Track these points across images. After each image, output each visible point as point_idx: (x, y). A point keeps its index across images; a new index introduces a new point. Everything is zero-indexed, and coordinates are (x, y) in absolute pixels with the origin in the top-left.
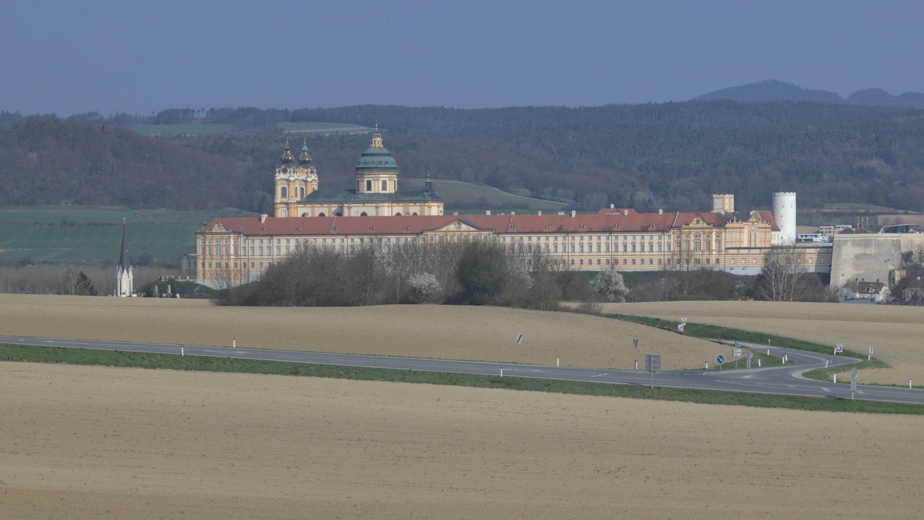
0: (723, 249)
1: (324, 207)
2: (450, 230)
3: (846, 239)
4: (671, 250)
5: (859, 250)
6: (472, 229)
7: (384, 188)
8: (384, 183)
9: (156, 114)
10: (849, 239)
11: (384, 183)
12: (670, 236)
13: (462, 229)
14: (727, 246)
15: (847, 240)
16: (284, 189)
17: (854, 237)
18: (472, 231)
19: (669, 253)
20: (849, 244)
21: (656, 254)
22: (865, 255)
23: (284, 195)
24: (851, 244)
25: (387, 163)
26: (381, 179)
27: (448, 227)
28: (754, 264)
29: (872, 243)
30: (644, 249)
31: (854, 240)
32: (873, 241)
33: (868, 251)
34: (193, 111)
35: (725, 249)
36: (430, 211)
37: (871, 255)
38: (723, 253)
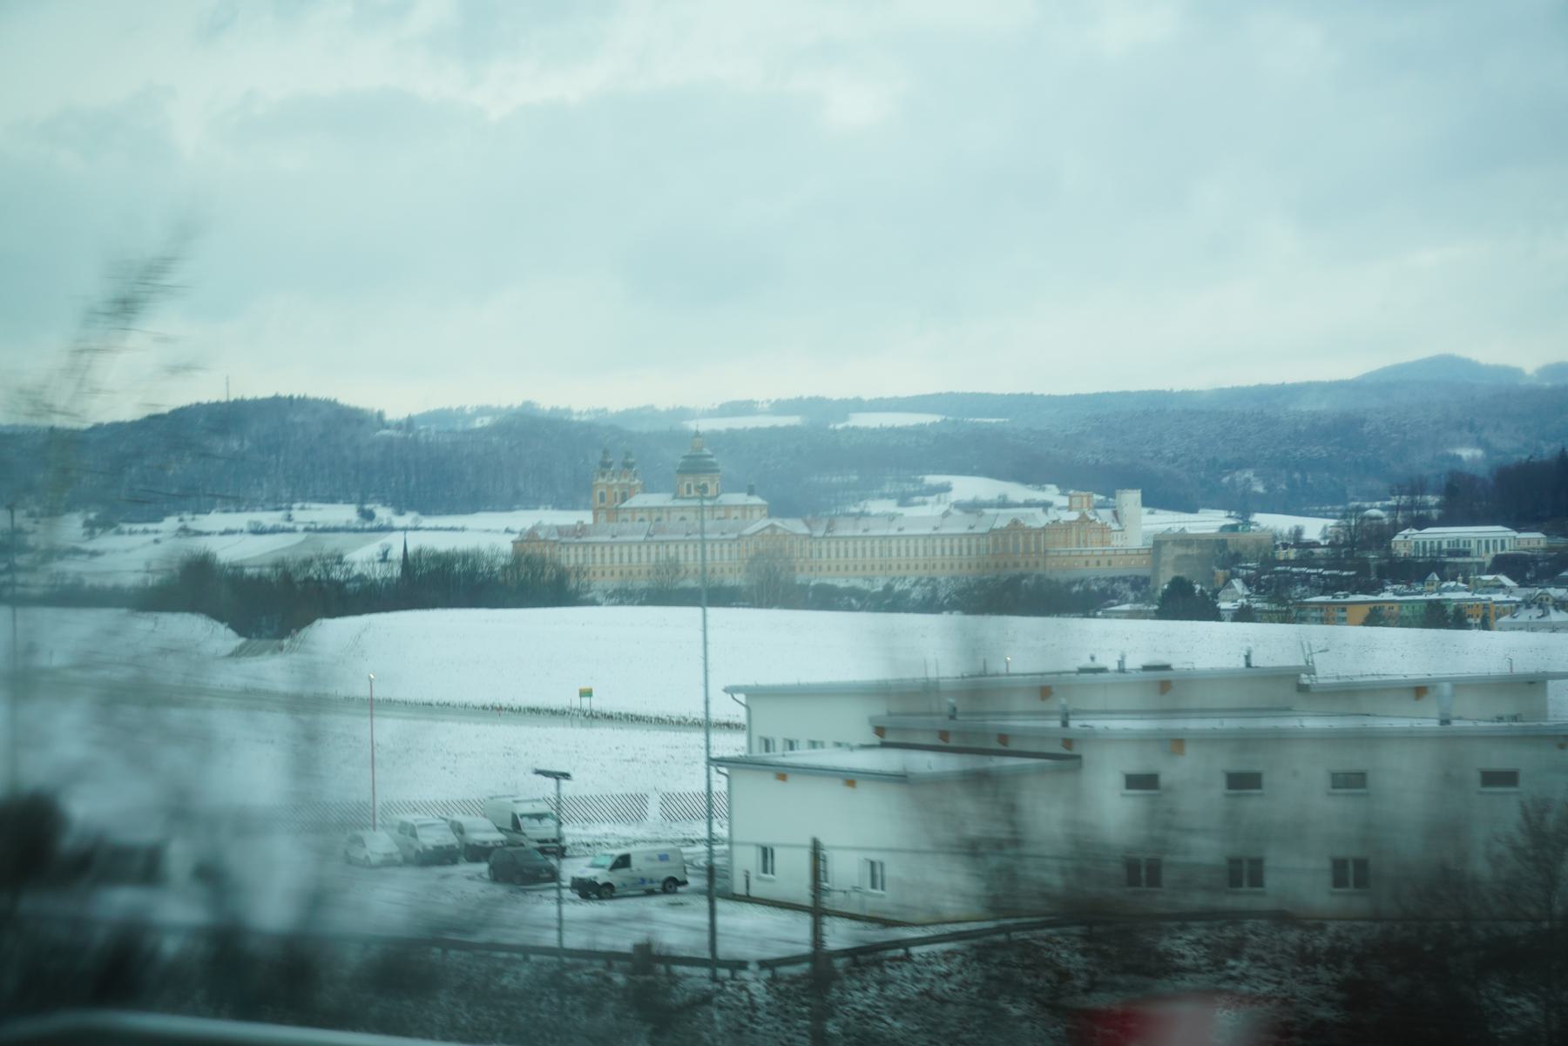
0: (1043, 550)
5: (1180, 551)
9: (716, 406)
16: (602, 495)
20: (1170, 544)
22: (1186, 556)
23: (602, 500)
33: (1190, 552)
34: (758, 403)
37: (1193, 555)
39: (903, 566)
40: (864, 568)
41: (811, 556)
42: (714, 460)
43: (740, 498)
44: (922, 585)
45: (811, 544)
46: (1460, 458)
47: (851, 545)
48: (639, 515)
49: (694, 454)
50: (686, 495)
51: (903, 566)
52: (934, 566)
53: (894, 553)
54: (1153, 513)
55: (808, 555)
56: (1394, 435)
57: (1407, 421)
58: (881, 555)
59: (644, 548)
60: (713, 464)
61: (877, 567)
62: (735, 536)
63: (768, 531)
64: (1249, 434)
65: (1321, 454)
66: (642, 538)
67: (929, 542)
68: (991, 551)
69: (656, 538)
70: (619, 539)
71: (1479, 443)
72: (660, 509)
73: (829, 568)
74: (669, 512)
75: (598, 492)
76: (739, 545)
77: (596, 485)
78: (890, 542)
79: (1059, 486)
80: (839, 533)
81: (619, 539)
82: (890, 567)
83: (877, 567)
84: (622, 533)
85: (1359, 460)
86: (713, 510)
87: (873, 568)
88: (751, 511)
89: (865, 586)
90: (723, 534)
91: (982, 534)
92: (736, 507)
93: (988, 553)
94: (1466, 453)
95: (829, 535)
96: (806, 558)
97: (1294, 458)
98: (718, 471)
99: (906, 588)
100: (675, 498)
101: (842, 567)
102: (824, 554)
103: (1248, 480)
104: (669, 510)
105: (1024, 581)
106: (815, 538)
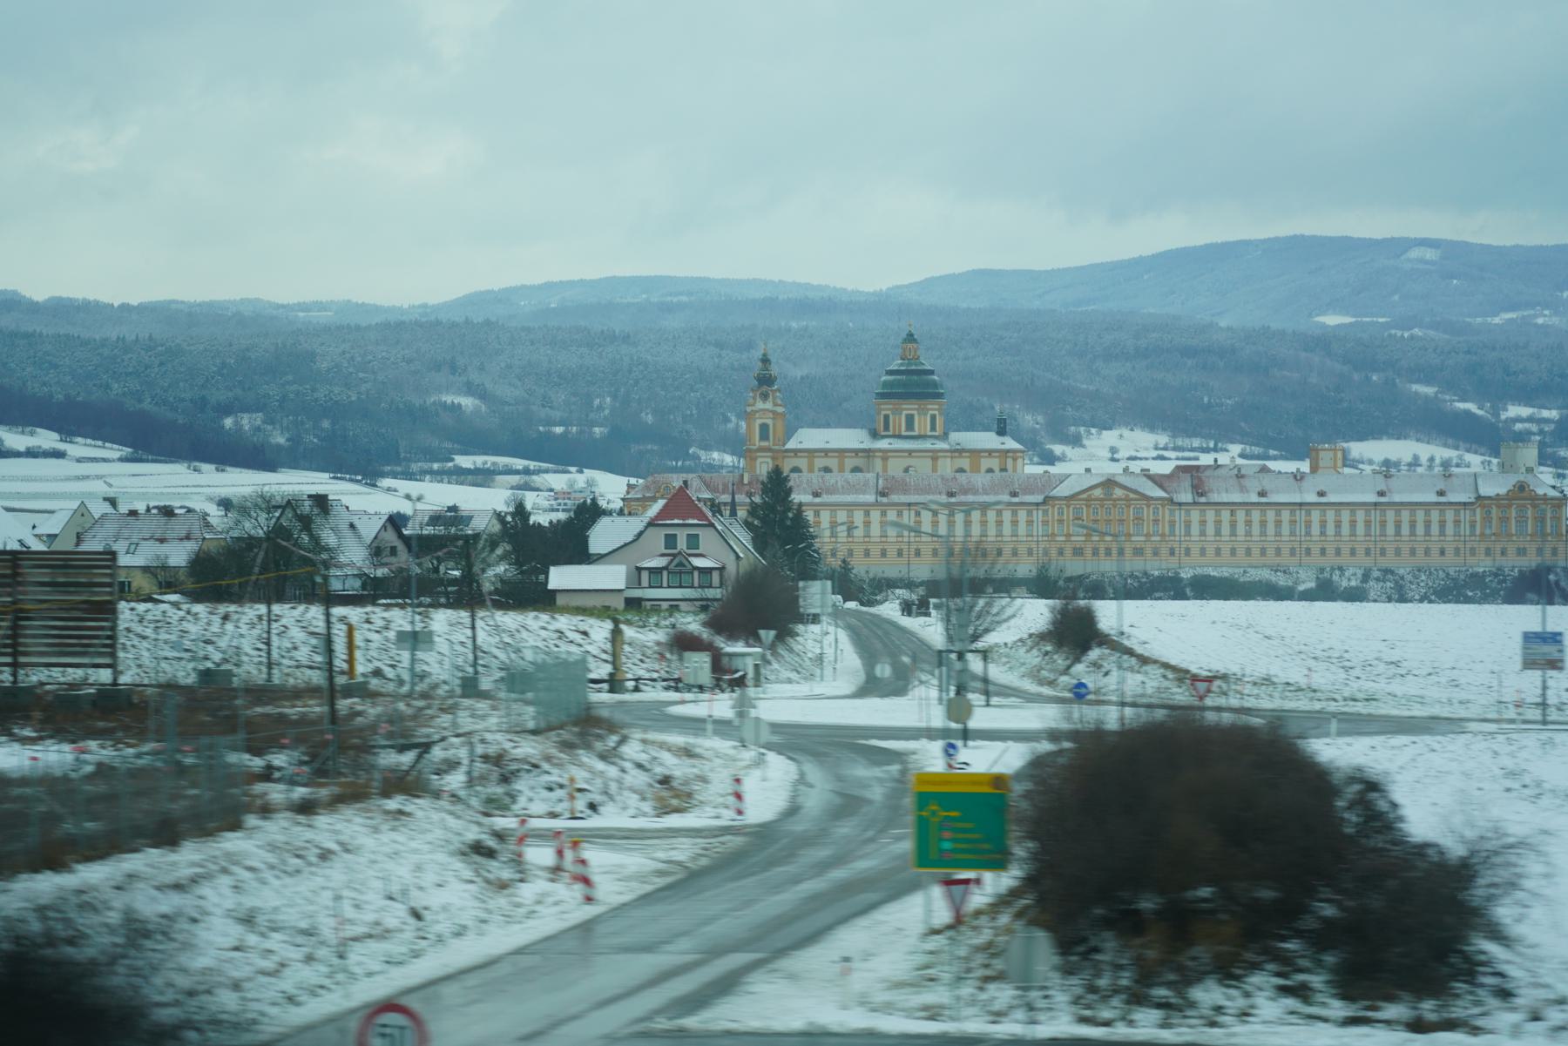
1: (801, 457)
4: (1478, 532)
6: (1132, 496)
8: (933, 418)
11: (933, 418)
13: (1115, 496)
16: (764, 427)
18: (1132, 499)
19: (1473, 538)
21: (1243, 538)
26: (905, 412)
30: (1400, 531)
38: (1564, 538)
39: (1330, 551)
40: (1263, 552)
41: (1172, 533)
42: (936, 378)
43: (987, 440)
44: (1378, 579)
45: (1172, 512)
46: (460, 405)
47: (1241, 515)
48: (820, 462)
49: (913, 368)
50: (904, 433)
51: (1330, 551)
52: (1383, 553)
53: (1315, 529)
54: (223, 471)
55: (1167, 531)
56: (361, 375)
57: (370, 357)
58: (1292, 534)
59: (875, 515)
60: (935, 385)
61: (1285, 552)
62: (1039, 498)
63: (1098, 493)
64: (147, 367)
65: (350, 396)
66: (870, 498)
67: (1375, 516)
68: (1478, 532)
69: (895, 498)
70: (825, 498)
71: (470, 389)
72: (856, 452)
73: (1203, 552)
74: (885, 459)
75: (759, 422)
76: (1045, 512)
77: (757, 412)
78: (1308, 513)
79: (59, 431)
80: (1215, 497)
81: (825, 498)
82: (1308, 552)
83: (1285, 552)
84: (831, 491)
85: (401, 406)
86: (952, 457)
87: (1278, 552)
88: (1015, 459)
89: (1282, 581)
90: (1014, 494)
91: (1465, 504)
92: (990, 452)
93: (1473, 534)
94: (467, 402)
95: (1203, 500)
96: (1163, 535)
97: (316, 400)
98: (940, 396)
99: (1353, 583)
100: (875, 435)
101: (1226, 551)
102: (1195, 529)
103: (258, 429)
104: (886, 455)
105: (1552, 577)
106: (1180, 504)
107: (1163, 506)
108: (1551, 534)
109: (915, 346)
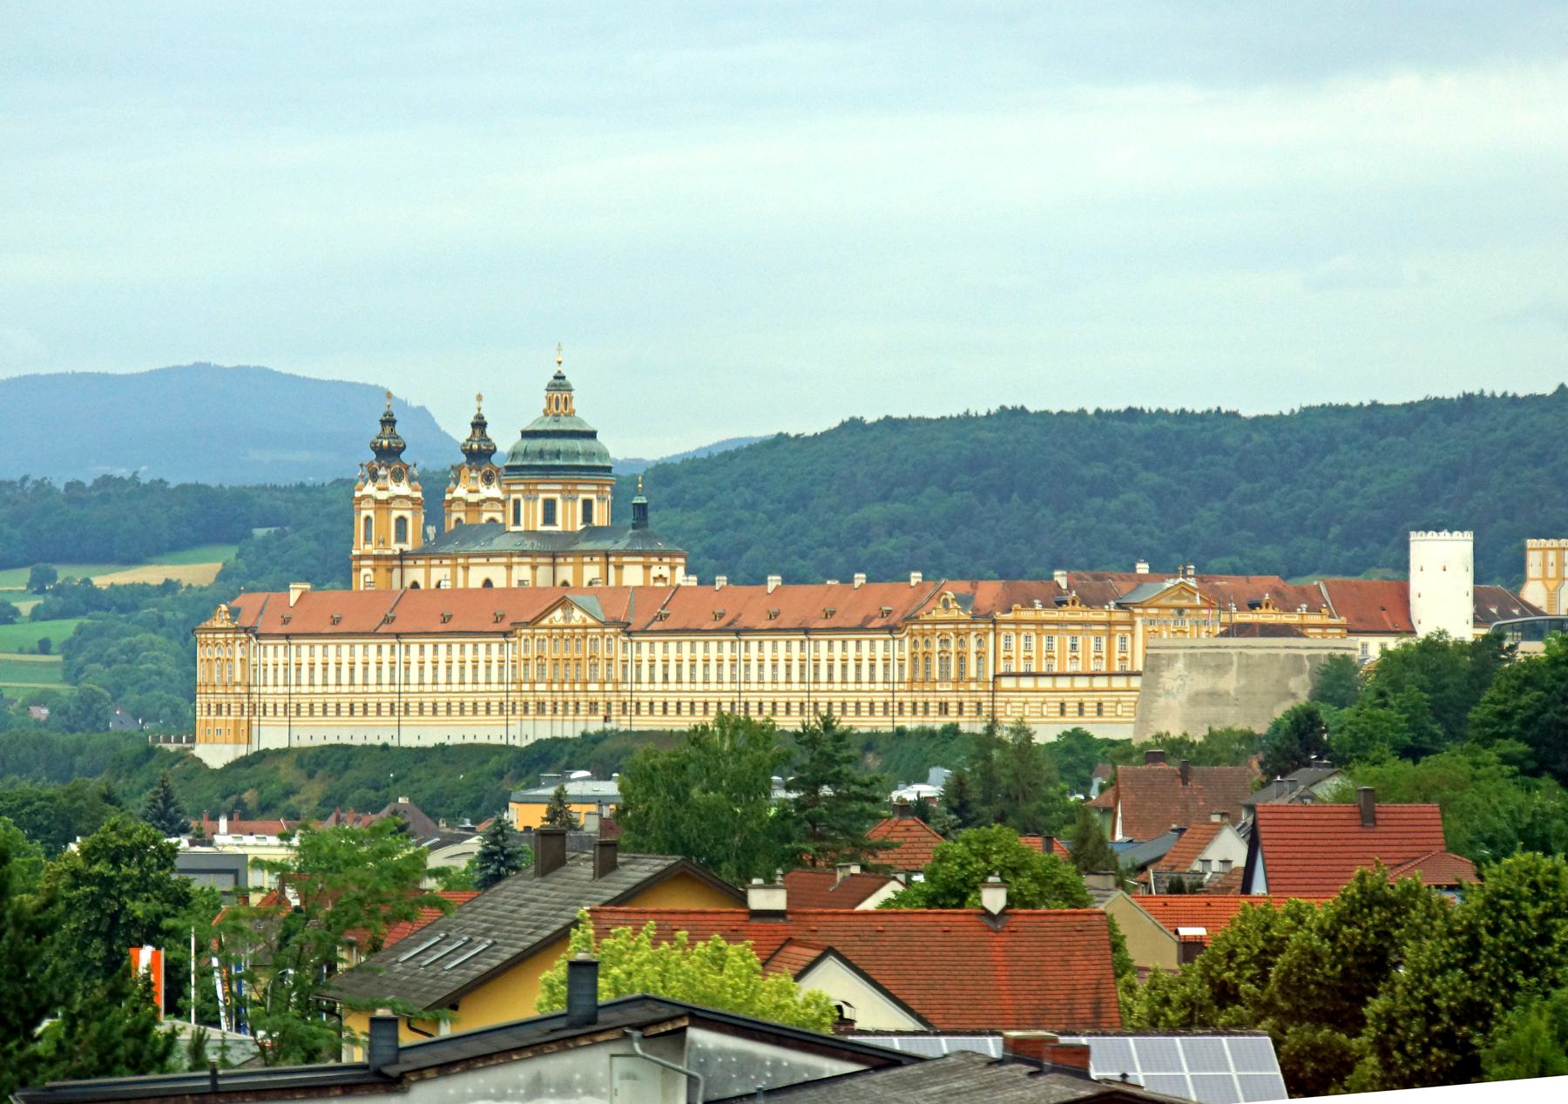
0: (991, 679)
2: (555, 623)
3: (1173, 651)
5: (1202, 682)
7: (549, 518)
8: (550, 506)
10: (1181, 652)
11: (550, 506)
12: (901, 640)
13: (573, 622)
14: (1002, 669)
15: (1176, 656)
17: (1192, 647)
19: (902, 686)
24: (1185, 665)
25: (558, 454)
27: (551, 616)
28: (1042, 716)
29: (1231, 663)
31: (1191, 655)
32: (1235, 659)
35: (995, 676)
36: (619, 578)
75: (364, 514)
86: (554, 565)
107: (616, 637)
108: (976, 680)
109: (565, 394)
